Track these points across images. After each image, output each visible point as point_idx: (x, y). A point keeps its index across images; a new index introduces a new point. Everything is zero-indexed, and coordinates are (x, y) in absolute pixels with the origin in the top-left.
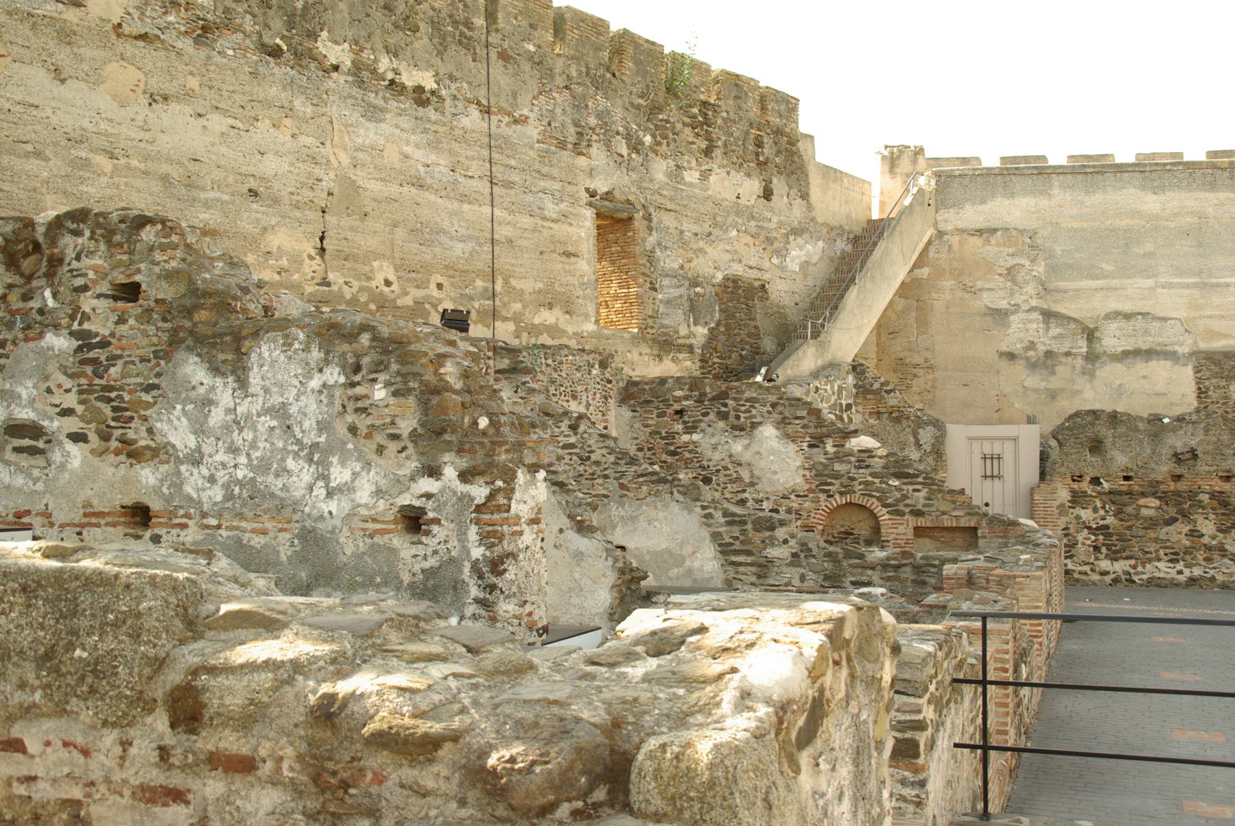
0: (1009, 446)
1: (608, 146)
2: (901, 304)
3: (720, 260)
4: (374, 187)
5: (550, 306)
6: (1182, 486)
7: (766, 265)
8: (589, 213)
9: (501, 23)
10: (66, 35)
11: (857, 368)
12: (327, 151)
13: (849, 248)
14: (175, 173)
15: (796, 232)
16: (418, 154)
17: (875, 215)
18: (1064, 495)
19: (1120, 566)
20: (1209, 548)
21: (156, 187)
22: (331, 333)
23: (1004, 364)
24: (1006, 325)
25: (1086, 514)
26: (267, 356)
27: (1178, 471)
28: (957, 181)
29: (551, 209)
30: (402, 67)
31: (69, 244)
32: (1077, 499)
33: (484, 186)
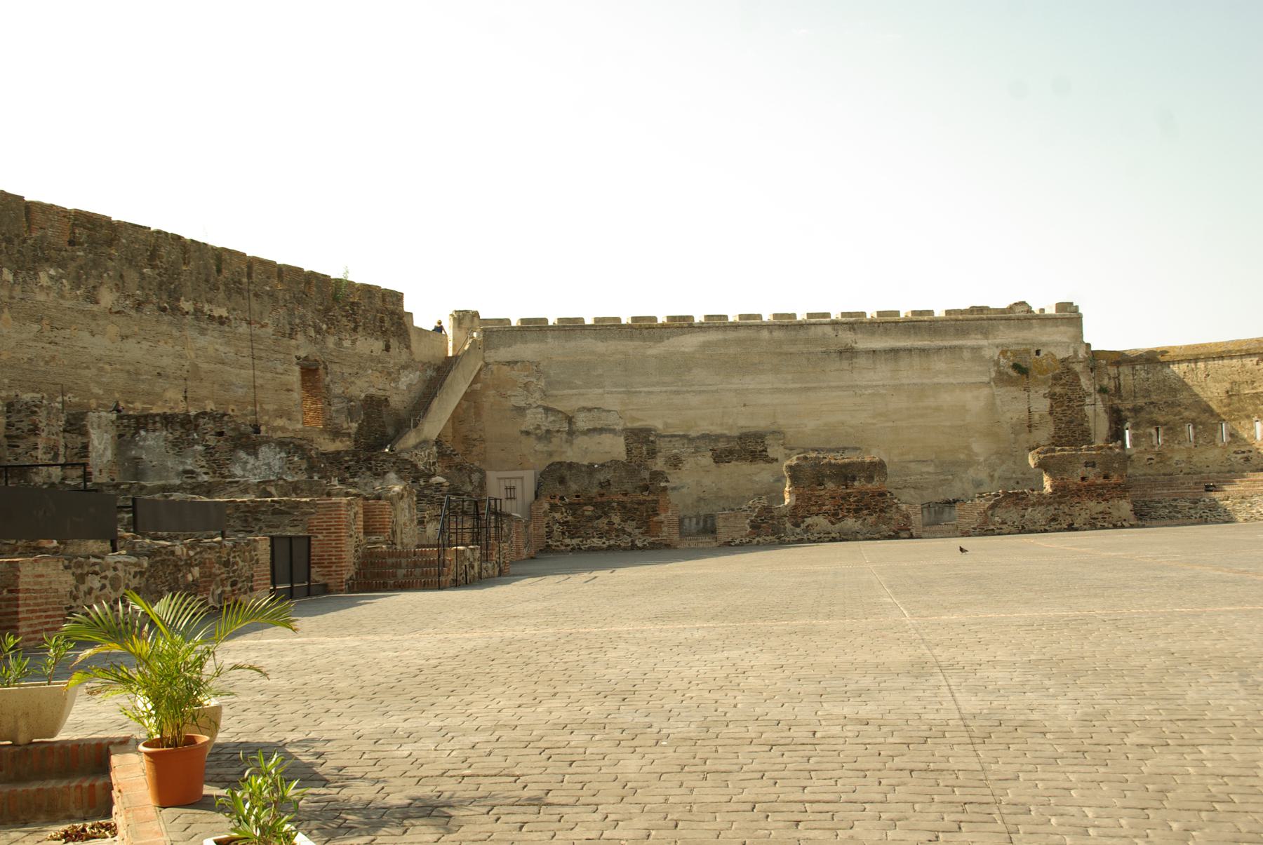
0: (519, 482)
1: (305, 332)
2: (465, 405)
3: (362, 387)
4: (205, 366)
5: (281, 417)
6: (604, 499)
7: (388, 387)
8: (297, 368)
9: (254, 279)
10: (94, 317)
11: (438, 443)
12: (186, 352)
13: (434, 374)
14: (131, 368)
15: (404, 368)
16: (221, 348)
17: (450, 354)
18: (546, 506)
19: (575, 541)
20: (617, 530)
21: (126, 376)
22: (281, 444)
23: (523, 438)
24: (525, 416)
25: (558, 516)
26: (264, 451)
27: (604, 491)
28: (497, 332)
29: (280, 368)
30: (213, 307)
31: (201, 421)
32: (553, 508)
33: (249, 360)
